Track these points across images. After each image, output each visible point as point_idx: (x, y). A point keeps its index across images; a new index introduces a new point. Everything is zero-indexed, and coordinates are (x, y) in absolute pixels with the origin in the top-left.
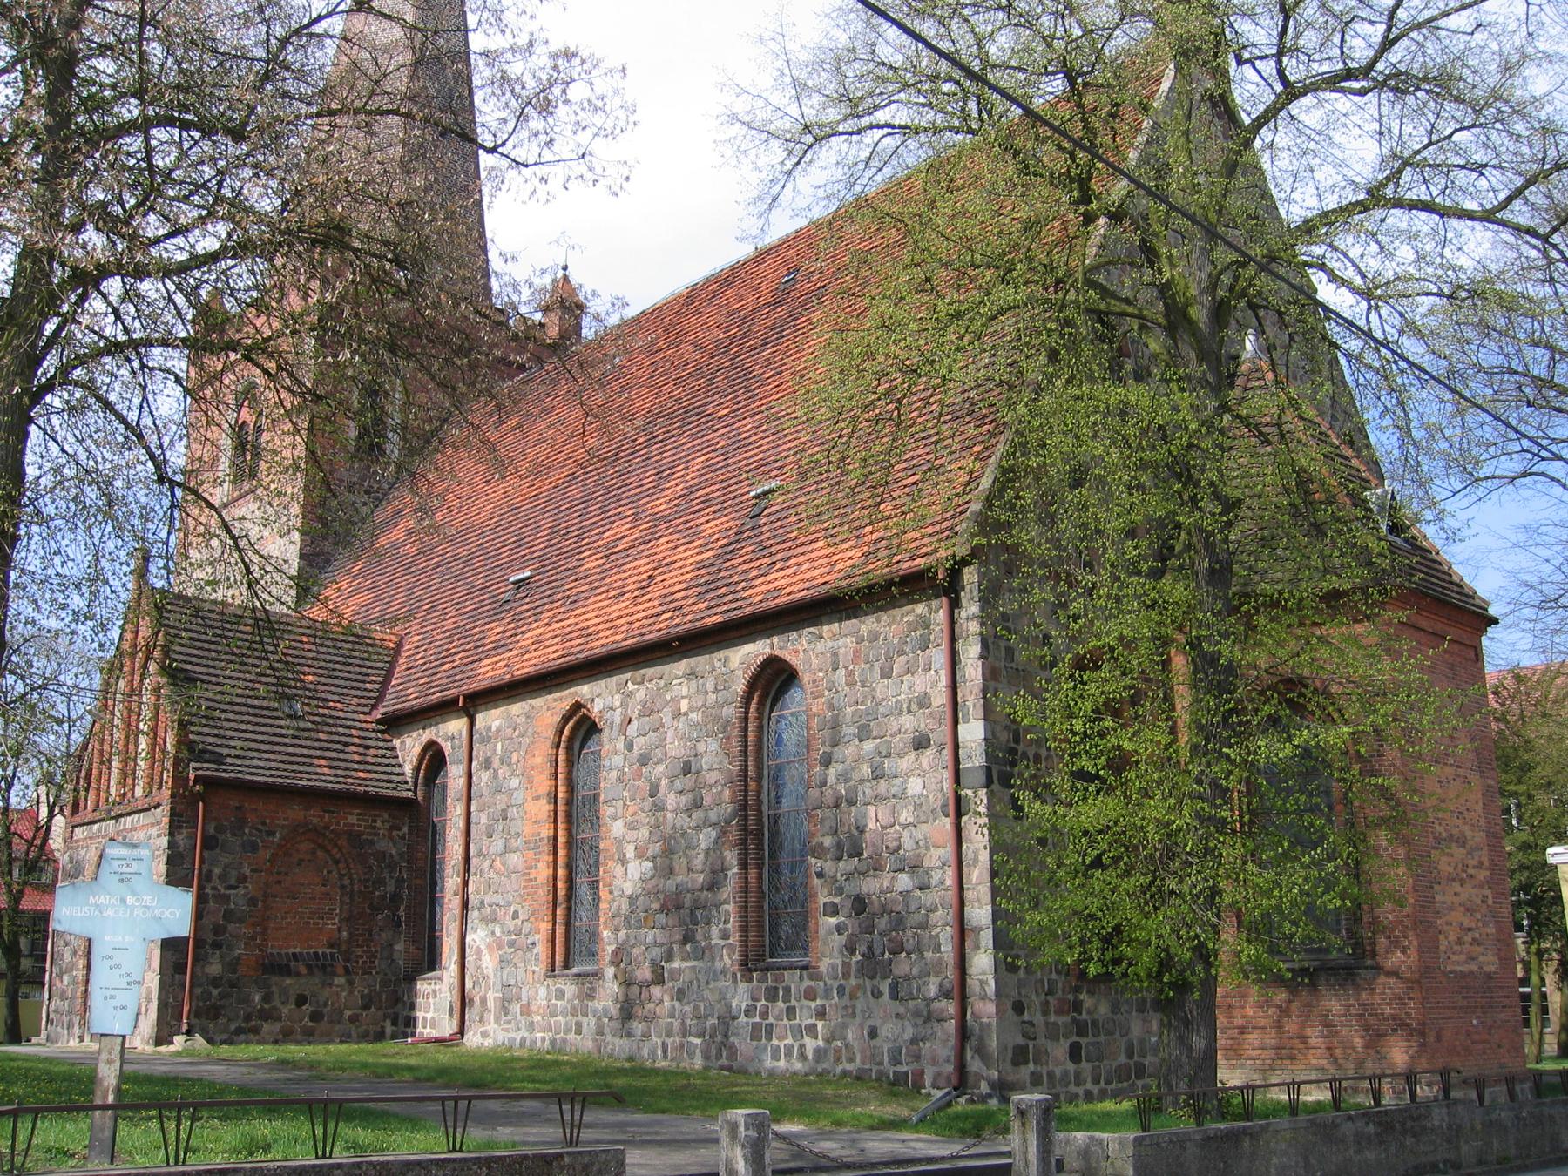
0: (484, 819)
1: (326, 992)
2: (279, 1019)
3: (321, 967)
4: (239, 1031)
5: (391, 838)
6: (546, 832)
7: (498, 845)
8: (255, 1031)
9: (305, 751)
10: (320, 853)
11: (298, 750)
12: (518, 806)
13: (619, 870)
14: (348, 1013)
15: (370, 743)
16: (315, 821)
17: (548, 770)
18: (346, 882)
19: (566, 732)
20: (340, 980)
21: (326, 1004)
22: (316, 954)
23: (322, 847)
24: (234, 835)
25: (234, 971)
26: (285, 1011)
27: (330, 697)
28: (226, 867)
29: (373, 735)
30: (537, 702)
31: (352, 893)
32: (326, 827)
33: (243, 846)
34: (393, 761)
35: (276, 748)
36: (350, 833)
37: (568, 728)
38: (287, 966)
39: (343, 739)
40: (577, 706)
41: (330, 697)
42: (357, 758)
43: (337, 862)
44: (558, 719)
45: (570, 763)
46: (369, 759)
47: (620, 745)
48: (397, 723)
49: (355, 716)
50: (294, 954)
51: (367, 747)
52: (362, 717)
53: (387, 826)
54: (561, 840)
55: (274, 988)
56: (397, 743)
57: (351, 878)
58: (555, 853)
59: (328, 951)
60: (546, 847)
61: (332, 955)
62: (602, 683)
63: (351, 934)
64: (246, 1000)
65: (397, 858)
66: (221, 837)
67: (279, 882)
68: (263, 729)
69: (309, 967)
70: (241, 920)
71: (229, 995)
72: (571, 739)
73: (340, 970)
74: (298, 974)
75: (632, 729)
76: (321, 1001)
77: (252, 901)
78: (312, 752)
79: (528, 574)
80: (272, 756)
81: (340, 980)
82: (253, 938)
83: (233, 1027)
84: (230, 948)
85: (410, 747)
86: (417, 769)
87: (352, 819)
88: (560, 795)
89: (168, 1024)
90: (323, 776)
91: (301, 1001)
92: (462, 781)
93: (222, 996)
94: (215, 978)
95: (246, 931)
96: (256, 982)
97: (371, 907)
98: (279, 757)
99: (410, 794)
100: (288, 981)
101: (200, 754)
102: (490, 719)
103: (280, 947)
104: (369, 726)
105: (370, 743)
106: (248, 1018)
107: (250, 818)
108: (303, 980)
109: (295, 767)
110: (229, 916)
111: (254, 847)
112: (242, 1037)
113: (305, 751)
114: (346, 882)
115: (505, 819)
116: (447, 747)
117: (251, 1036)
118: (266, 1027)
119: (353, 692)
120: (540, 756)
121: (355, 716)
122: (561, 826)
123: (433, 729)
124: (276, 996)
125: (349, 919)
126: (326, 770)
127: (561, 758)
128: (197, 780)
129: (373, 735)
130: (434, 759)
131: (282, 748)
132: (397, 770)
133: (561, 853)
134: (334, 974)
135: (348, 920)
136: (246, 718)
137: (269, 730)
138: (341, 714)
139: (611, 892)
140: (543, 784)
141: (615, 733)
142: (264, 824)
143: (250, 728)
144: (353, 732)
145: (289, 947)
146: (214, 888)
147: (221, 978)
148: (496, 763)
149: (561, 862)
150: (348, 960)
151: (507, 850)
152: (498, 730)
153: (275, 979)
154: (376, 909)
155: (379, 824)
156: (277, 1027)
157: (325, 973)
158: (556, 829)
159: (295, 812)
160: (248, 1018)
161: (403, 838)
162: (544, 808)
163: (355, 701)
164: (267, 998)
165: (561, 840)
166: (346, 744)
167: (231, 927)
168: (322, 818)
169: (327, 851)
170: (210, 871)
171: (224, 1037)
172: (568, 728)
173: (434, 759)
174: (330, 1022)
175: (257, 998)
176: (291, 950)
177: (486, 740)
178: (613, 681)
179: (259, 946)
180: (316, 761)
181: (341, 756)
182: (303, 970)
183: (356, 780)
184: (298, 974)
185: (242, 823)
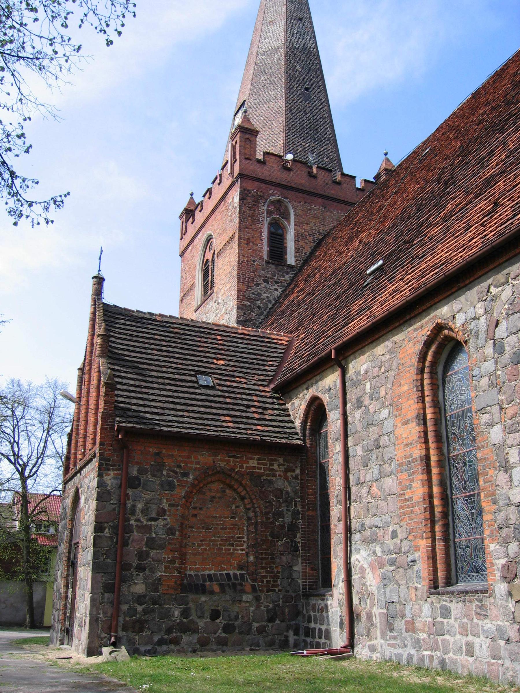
0: (359, 451)
1: (236, 608)
2: (195, 631)
3: (232, 585)
4: (161, 642)
5: (286, 478)
6: (418, 452)
7: (374, 471)
8: (176, 642)
9: (214, 411)
10: (228, 491)
11: (208, 410)
12: (388, 434)
13: (502, 477)
14: (255, 625)
15: (268, 406)
16: (222, 464)
17: (415, 395)
18: (251, 515)
19: (429, 358)
20: (248, 597)
21: (237, 618)
22: (228, 575)
23: (230, 487)
24: (154, 476)
25: (156, 590)
26: (201, 624)
27: (236, 374)
28: (147, 502)
29: (270, 400)
30: (398, 338)
31: (256, 523)
32: (232, 470)
33: (162, 485)
34: (286, 419)
35: (190, 408)
36: (251, 474)
37: (430, 353)
38: (203, 586)
39: (245, 403)
40: (439, 328)
41: (236, 374)
42: (256, 416)
43: (243, 499)
44: (420, 346)
45: (434, 385)
46: (267, 417)
47: (489, 350)
48: (287, 389)
49: (256, 387)
50: (209, 575)
51: (266, 409)
52: (261, 388)
53: (282, 468)
54: (434, 458)
55: (191, 605)
56: (289, 405)
57: (254, 511)
58: (429, 471)
59: (238, 572)
60: (419, 467)
61: (242, 575)
62: (462, 298)
63: (256, 558)
64: (167, 615)
65: (292, 494)
66: (143, 478)
67: (195, 516)
68: (181, 395)
69: (221, 586)
70: (161, 547)
71: (153, 611)
72: (434, 364)
73: (248, 588)
74: (212, 593)
75: (501, 332)
76: (233, 615)
77: (171, 531)
78: (220, 412)
79: (381, 262)
80: (186, 414)
81: (248, 597)
82: (172, 562)
83: (156, 639)
84: (153, 571)
85: (298, 406)
86: (304, 423)
87: (253, 463)
88: (429, 416)
89: (99, 637)
90: (228, 427)
91: (215, 615)
92: (339, 423)
93: (146, 612)
94: (140, 596)
95: (165, 556)
96: (175, 600)
97: (272, 535)
98: (192, 415)
99: (299, 442)
100: (203, 599)
101: (124, 412)
102: (360, 365)
103: (198, 570)
104: (267, 394)
105: (268, 406)
106: (169, 631)
107: (168, 462)
108: (216, 598)
109: (205, 422)
110: (151, 543)
111: (171, 486)
112: (165, 647)
113: (214, 411)
114: (251, 515)
115: (378, 447)
116: (325, 398)
117: (172, 647)
118: (185, 638)
119: (255, 372)
120: (407, 385)
121: (256, 387)
122: (432, 445)
123: (314, 388)
124: (193, 611)
125: (254, 546)
126: (230, 425)
127: (426, 382)
128: (120, 429)
129: (270, 400)
130: (317, 412)
131: (195, 409)
132: (290, 425)
133: (435, 471)
134: (243, 592)
135: (253, 546)
136: (168, 387)
137: (186, 395)
138: (245, 386)
139: (495, 502)
140: (411, 407)
141: (481, 340)
142: (179, 467)
143: (170, 394)
144: (254, 398)
145: (204, 569)
146: (138, 520)
147: (144, 596)
148: (366, 401)
149: (435, 479)
150: (254, 580)
151: (382, 475)
152: (366, 372)
153: (191, 596)
154: (276, 536)
155: (276, 467)
156: (195, 638)
157: (235, 590)
158: (427, 449)
159: (204, 458)
160: (169, 631)
161: (296, 478)
162: (414, 430)
163: (257, 377)
164: (185, 613)
165: (434, 458)
166: (249, 406)
167: (153, 553)
168: (228, 462)
169: (235, 490)
170: (134, 506)
171: (149, 647)
172: (430, 353)
173: (317, 412)
174: (241, 633)
175: (176, 613)
176: (207, 572)
177: (356, 385)
178: (473, 293)
179: (176, 569)
180: (222, 418)
181: (244, 414)
182: (216, 588)
183: (255, 432)
184: (212, 593)
185: (161, 466)
